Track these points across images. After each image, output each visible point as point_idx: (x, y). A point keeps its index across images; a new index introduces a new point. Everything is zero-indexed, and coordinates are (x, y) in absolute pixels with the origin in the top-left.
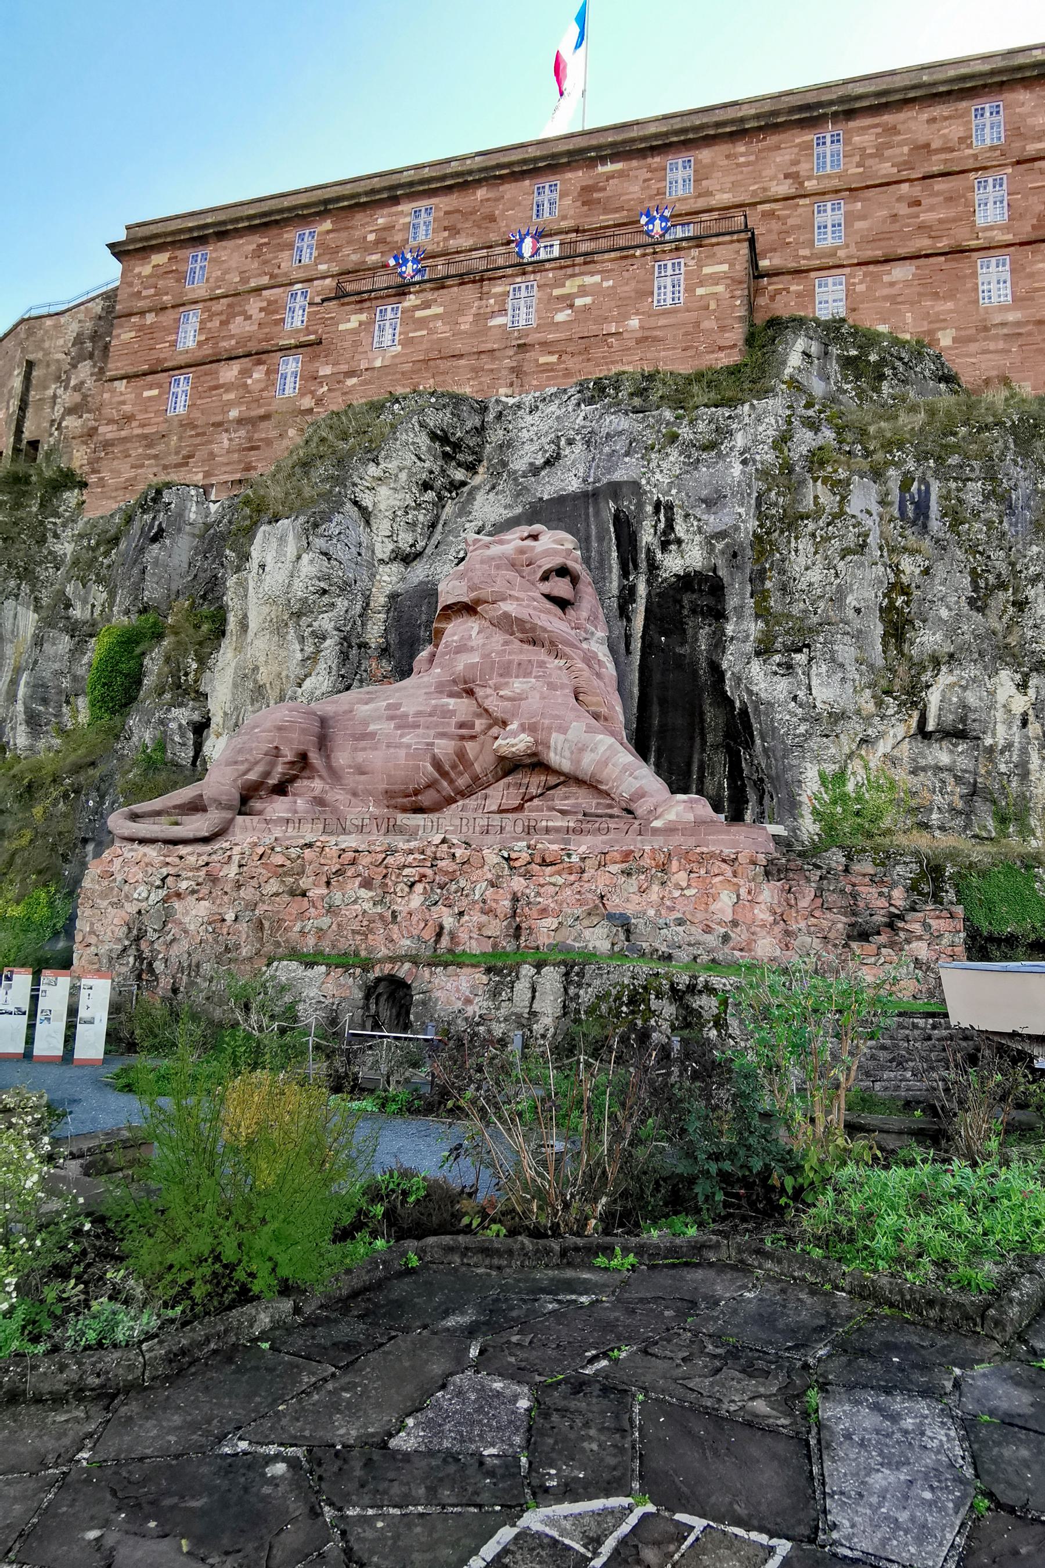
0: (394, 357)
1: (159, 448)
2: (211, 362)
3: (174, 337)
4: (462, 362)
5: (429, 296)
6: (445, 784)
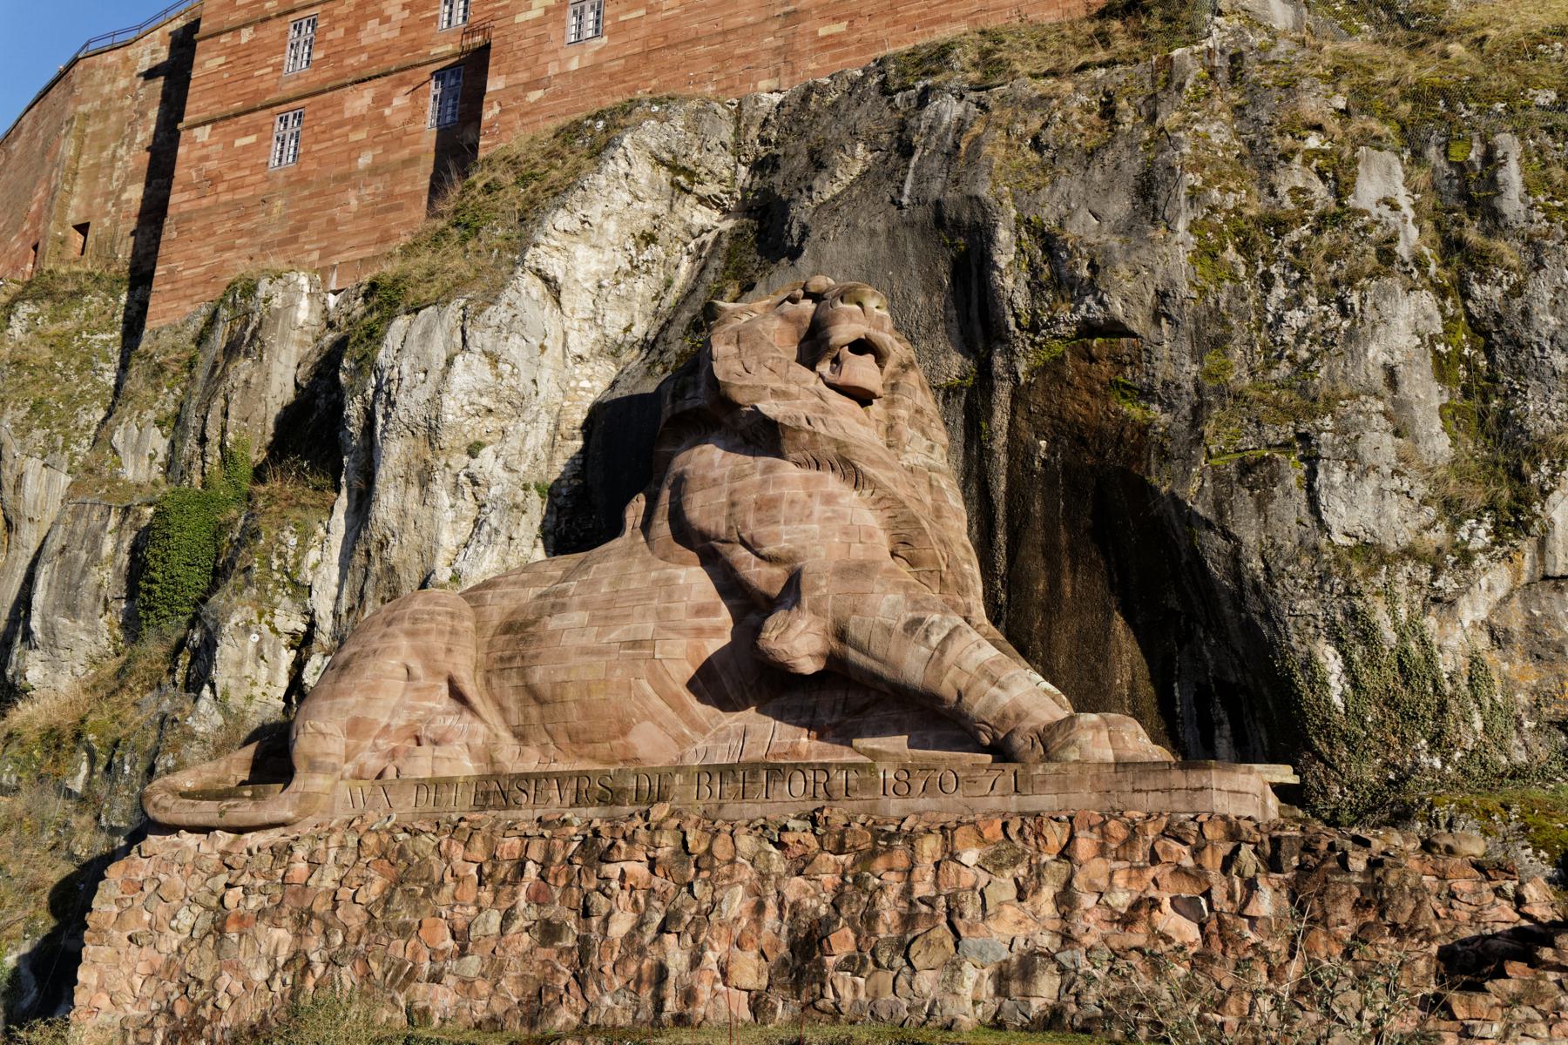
0: (597, 53)
2: (332, 89)
4: (701, 49)
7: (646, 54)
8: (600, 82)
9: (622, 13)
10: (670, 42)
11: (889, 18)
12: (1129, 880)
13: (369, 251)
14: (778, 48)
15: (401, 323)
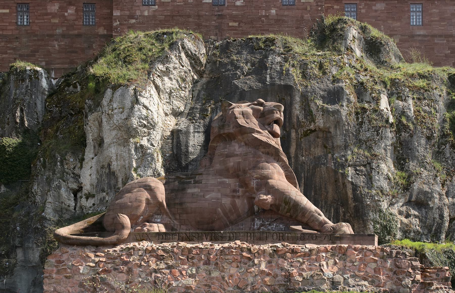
6: (225, 219)
14: (216, 26)
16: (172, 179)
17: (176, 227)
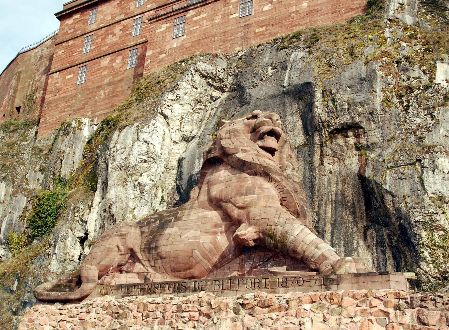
0: (183, 41)
1: (72, 102)
3: (81, 49)
4: (217, 38)
5: (200, 9)
6: (206, 262)
7: (198, 41)
8: (183, 51)
9: (191, 28)
10: (206, 36)
11: (279, 25)
12: (362, 312)
13: (108, 111)
14: (242, 36)
15: (117, 133)
16: (154, 218)
17: (148, 277)
